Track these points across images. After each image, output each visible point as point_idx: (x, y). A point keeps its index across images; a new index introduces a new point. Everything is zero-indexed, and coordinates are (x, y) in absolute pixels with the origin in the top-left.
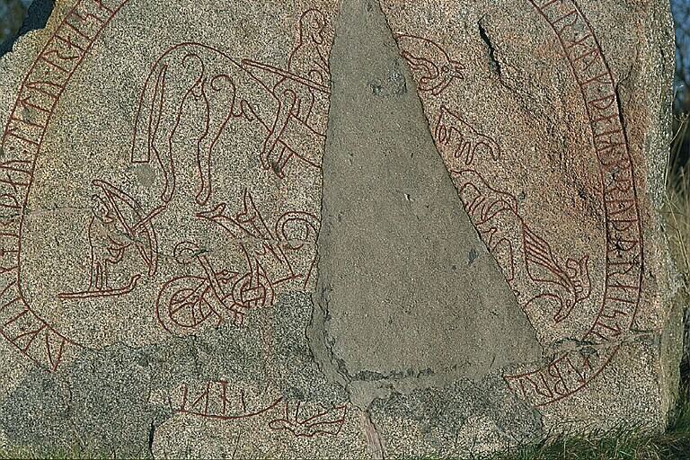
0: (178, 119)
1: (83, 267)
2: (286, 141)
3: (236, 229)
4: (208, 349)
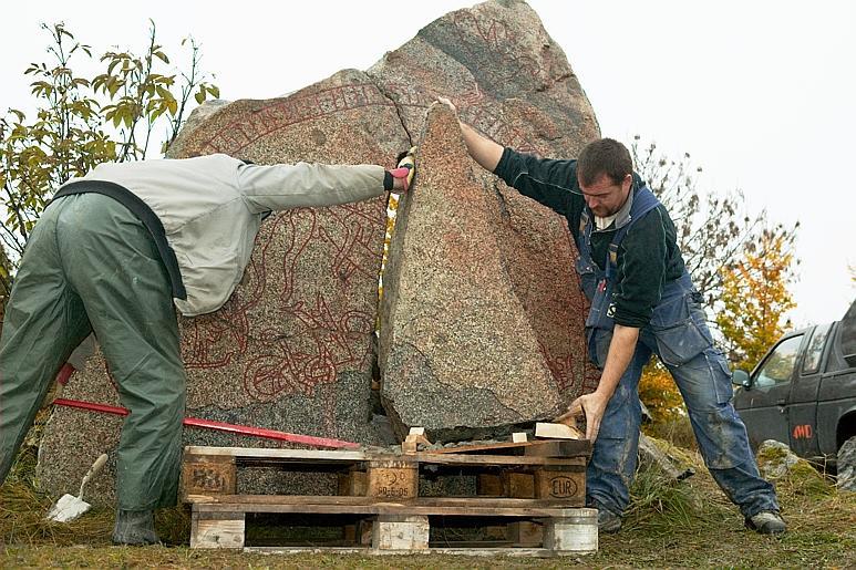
0: (271, 238)
1: (189, 344)
2: (352, 258)
3: (310, 322)
4: (283, 414)
